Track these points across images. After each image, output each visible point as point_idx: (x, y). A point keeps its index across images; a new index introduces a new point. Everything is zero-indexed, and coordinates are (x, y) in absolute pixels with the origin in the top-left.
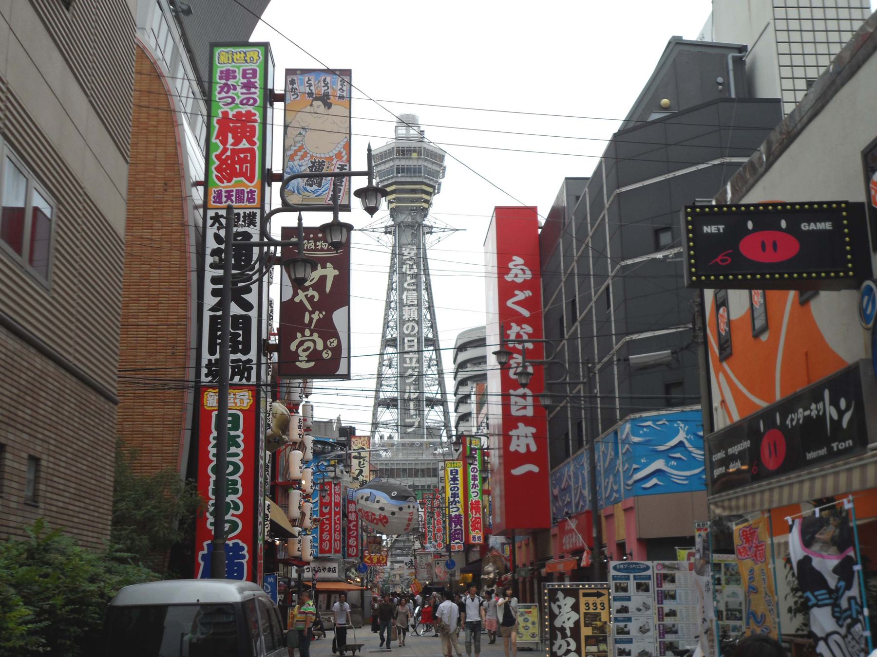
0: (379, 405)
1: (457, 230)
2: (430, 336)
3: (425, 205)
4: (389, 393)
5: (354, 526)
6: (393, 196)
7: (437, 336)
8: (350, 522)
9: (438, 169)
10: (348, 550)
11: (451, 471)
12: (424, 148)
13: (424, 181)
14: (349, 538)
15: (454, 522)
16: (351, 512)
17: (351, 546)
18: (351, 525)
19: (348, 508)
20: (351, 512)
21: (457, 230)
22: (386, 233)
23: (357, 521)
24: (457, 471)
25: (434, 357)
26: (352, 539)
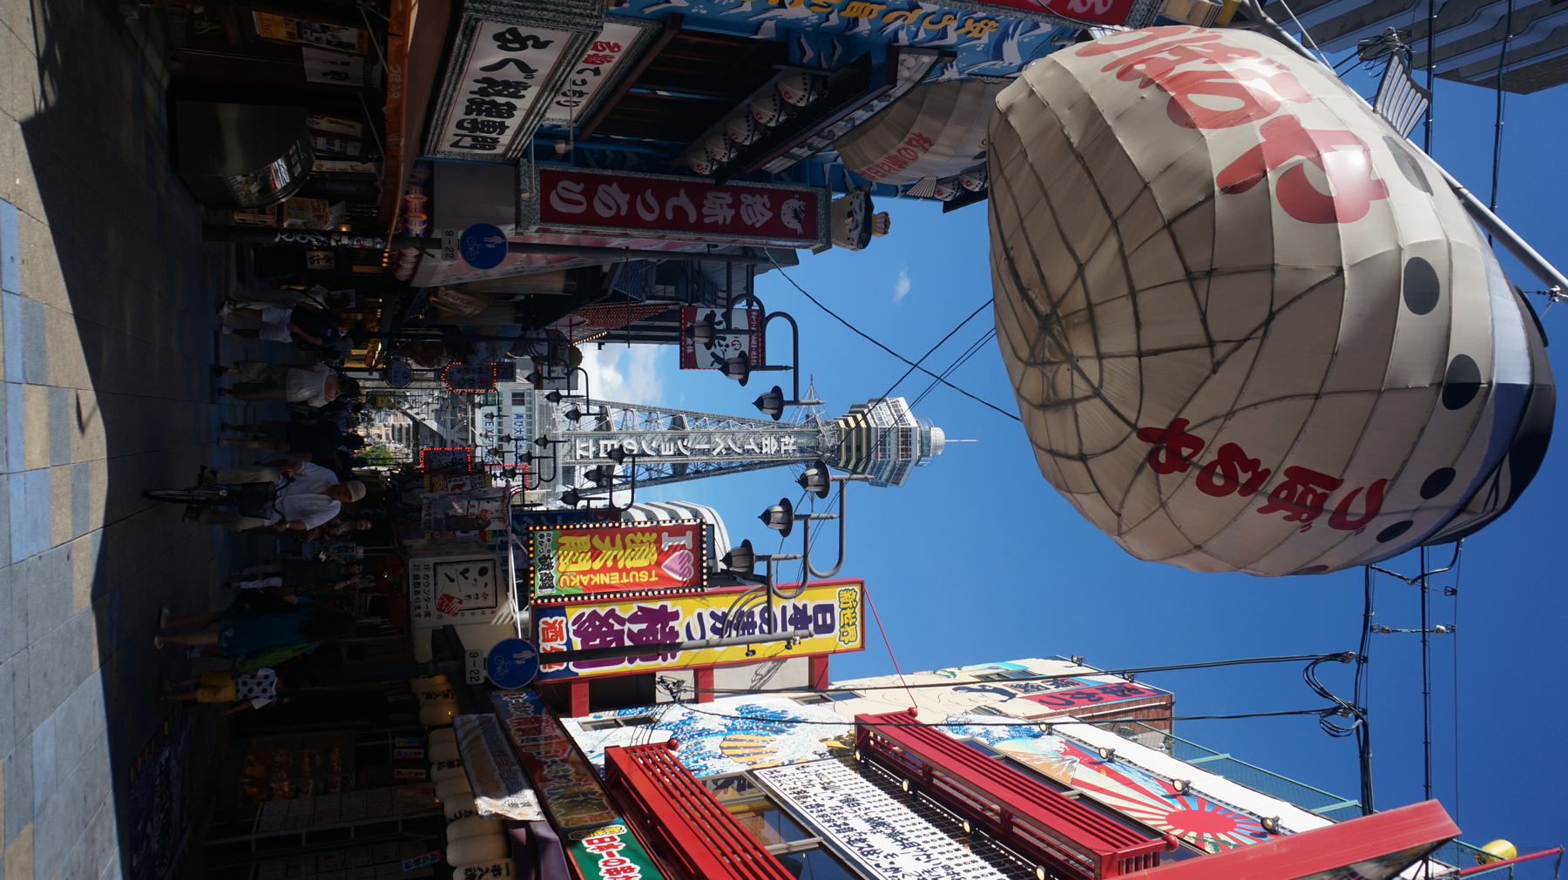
0: (600, 407)
1: (812, 502)
2: (688, 471)
3: (842, 464)
4: (614, 416)
5: (679, 210)
6: (853, 425)
7: (688, 479)
8: (698, 200)
9: (884, 478)
10: (575, 178)
11: (830, 608)
12: (910, 461)
13: (872, 462)
14: (625, 185)
15: (651, 631)
16: (736, 205)
17: (589, 194)
18: (683, 200)
19: (753, 192)
20: (736, 205)
21: (812, 502)
22: (807, 417)
23: (701, 227)
24: (829, 629)
25: (663, 475)
26: (623, 199)
